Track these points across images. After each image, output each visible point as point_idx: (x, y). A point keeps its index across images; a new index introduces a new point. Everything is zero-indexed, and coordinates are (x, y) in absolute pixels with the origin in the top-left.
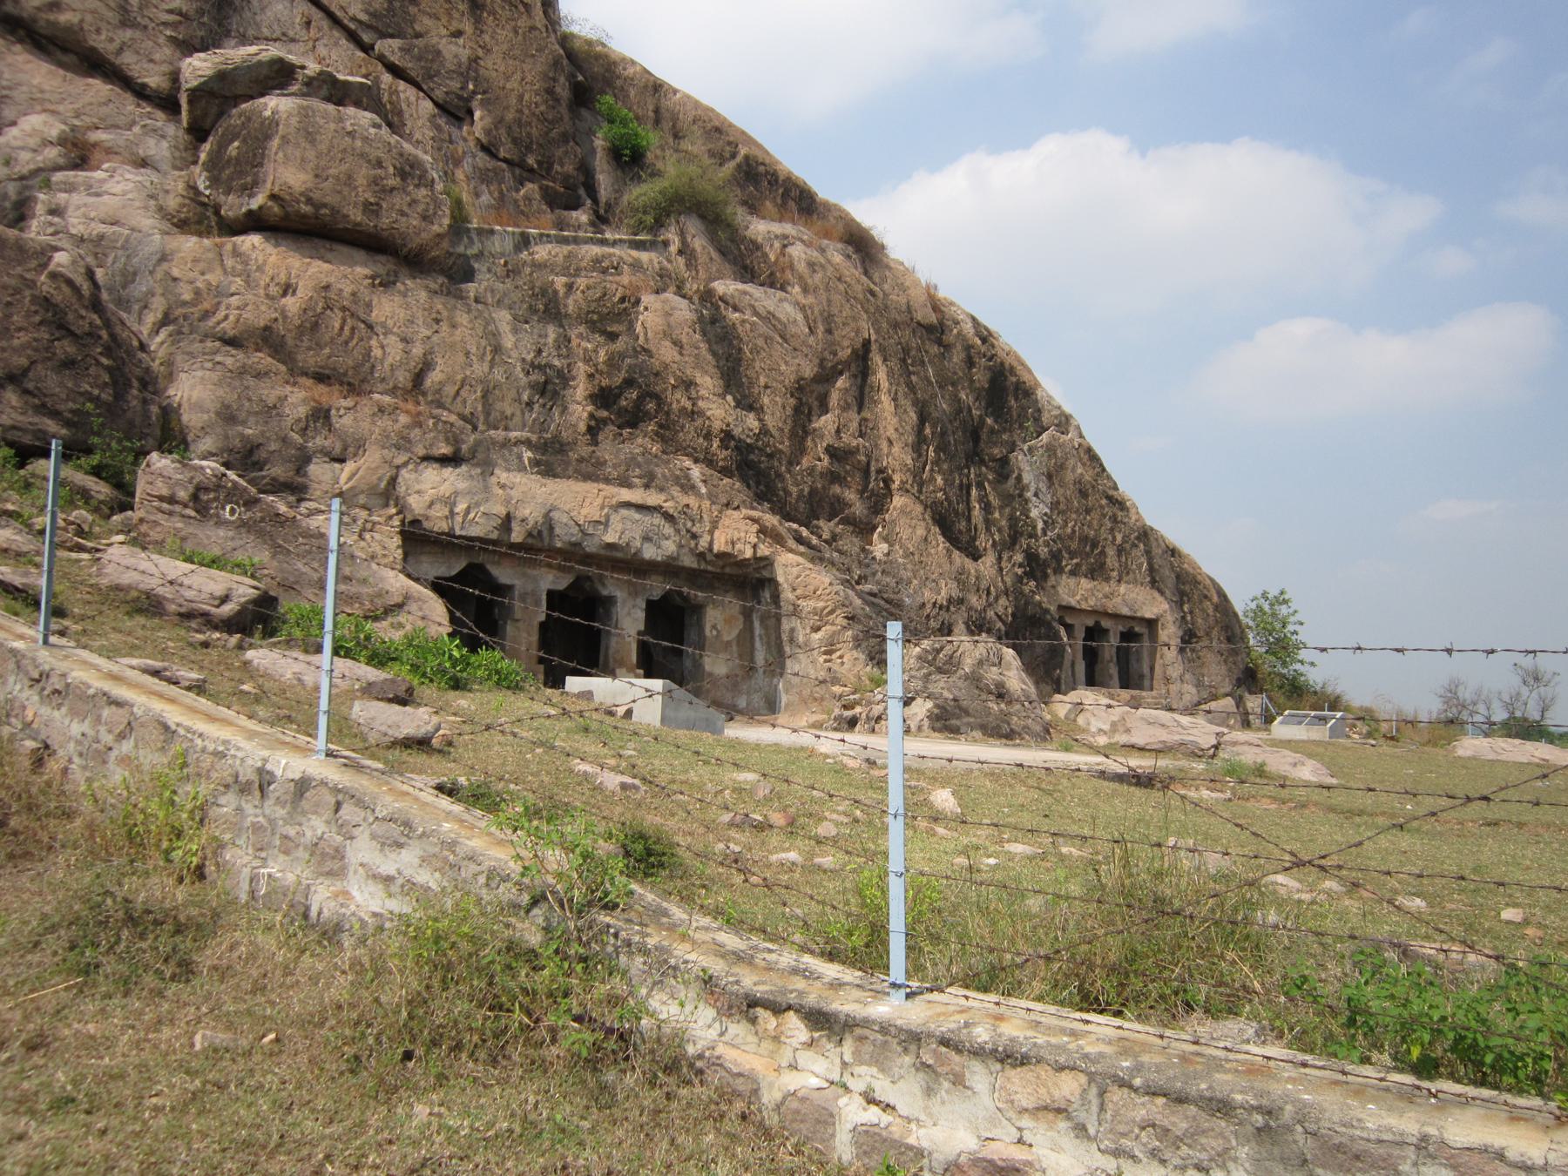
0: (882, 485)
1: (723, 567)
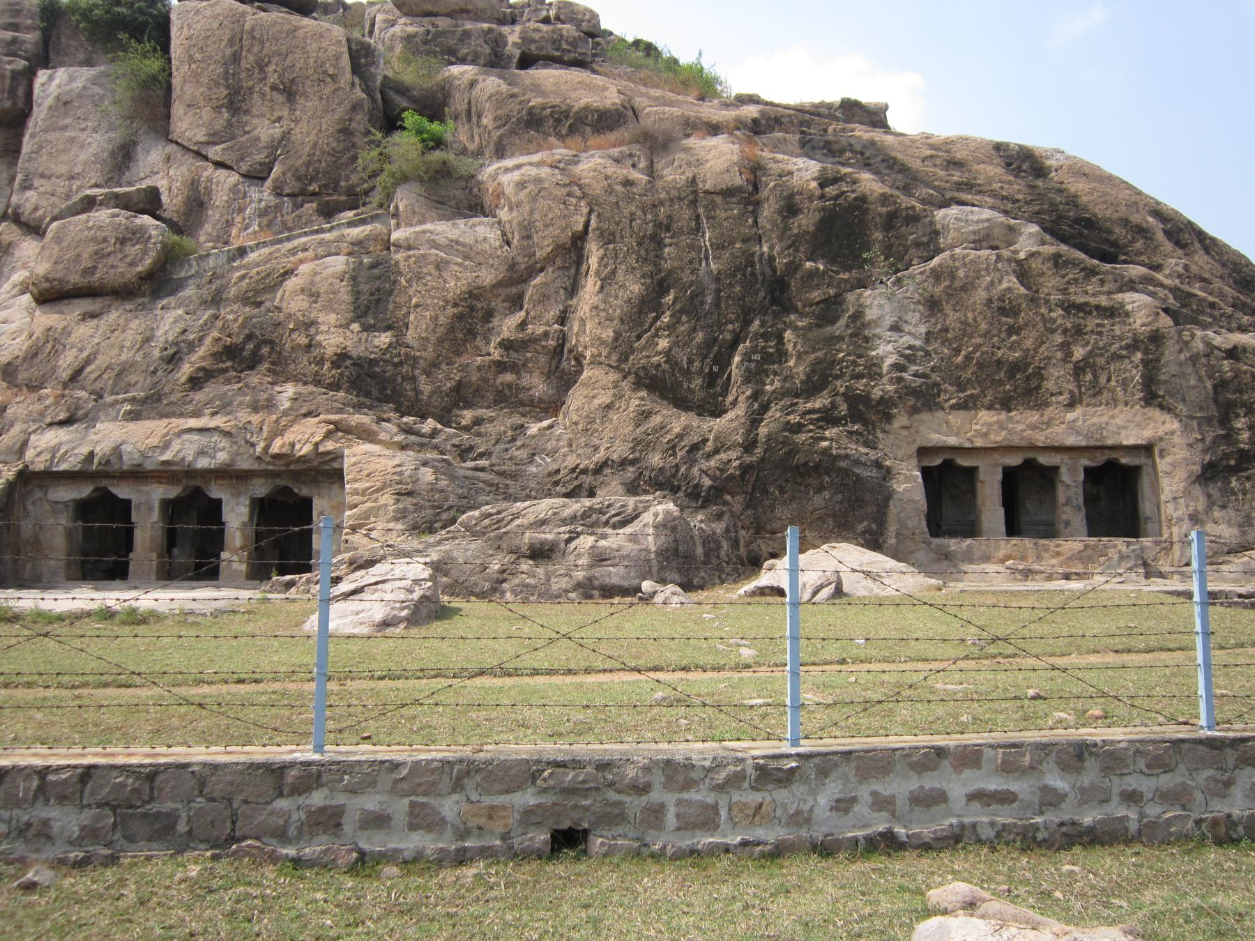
0: (573, 363)
1: (288, 465)
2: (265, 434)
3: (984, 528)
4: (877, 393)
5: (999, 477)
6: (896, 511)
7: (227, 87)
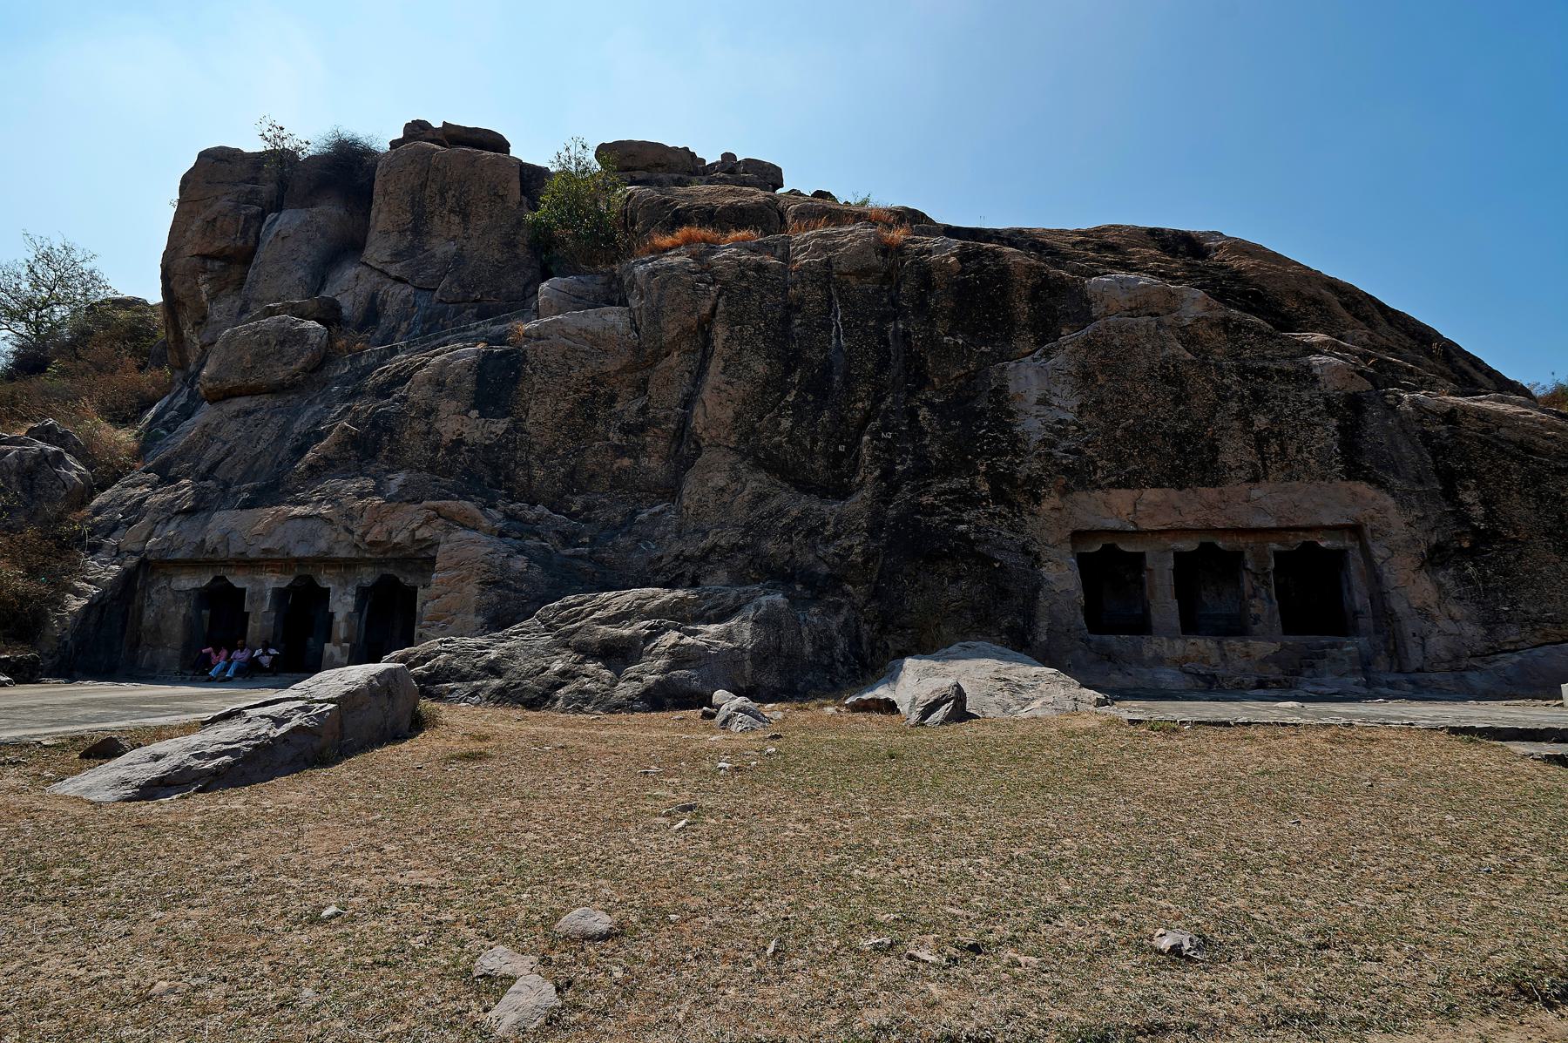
0: (692, 446)
1: (385, 552)
2: (365, 520)
3: (1154, 624)
4: (1023, 471)
5: (1171, 564)
6: (1046, 604)
7: (413, 214)
